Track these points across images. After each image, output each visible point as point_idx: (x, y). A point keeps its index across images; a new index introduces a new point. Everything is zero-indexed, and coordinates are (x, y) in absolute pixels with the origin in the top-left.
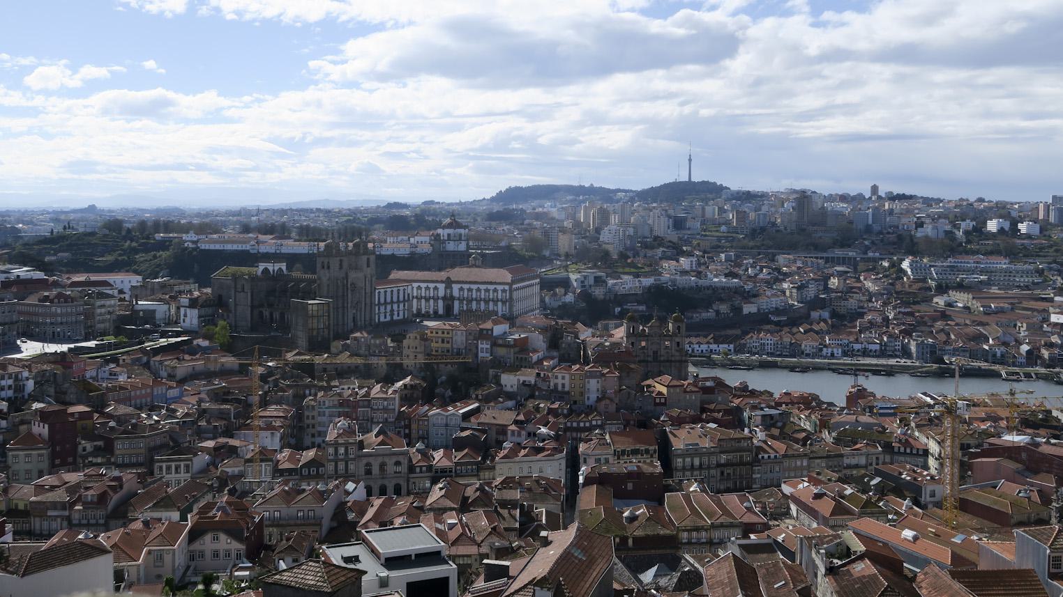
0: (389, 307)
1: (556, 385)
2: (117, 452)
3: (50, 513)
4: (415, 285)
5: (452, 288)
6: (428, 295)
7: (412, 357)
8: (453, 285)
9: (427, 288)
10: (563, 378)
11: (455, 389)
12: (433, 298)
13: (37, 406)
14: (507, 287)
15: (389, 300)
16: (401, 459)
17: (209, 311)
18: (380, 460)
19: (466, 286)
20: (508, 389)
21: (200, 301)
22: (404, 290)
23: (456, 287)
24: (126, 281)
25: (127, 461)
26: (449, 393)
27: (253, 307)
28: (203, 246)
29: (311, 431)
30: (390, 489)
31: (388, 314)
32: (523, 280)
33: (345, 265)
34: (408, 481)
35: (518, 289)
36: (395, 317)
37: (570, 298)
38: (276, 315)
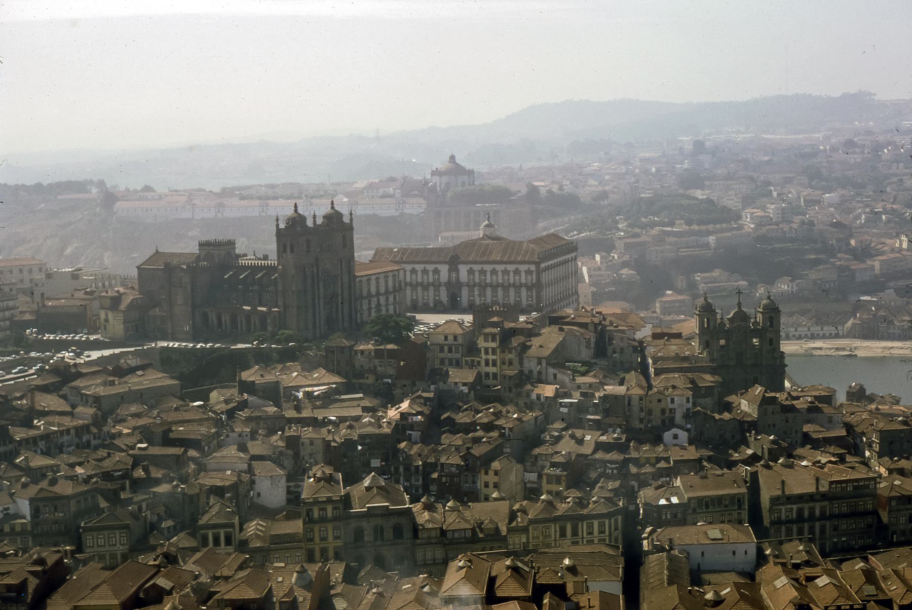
5: (457, 271)
6: (425, 280)
8: (461, 267)
9: (425, 272)
12: (433, 284)
14: (533, 268)
19: (476, 267)
22: (394, 275)
23: (463, 269)
31: (373, 311)
35: (548, 268)
38: (226, 318)
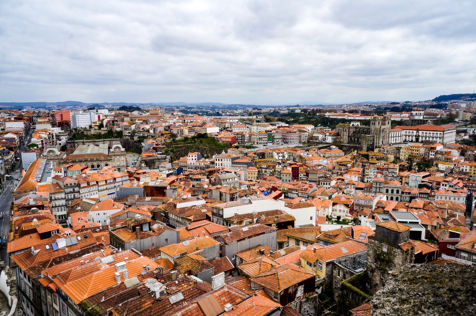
0: (395, 138)
1: (463, 170)
2: (309, 177)
3: (293, 192)
4: (405, 131)
7: (403, 155)
9: (409, 132)
10: (466, 167)
11: (419, 167)
13: (288, 162)
15: (395, 136)
16: (399, 189)
17: (335, 137)
18: (391, 189)
19: (425, 132)
20: (441, 169)
21: (332, 134)
24: (309, 128)
25: (312, 180)
26: (417, 169)
27: (349, 136)
28: (331, 117)
29: (367, 177)
30: (394, 199)
32: (449, 130)
33: (380, 123)
34: (401, 196)
36: (397, 142)
37: (467, 137)
38: (356, 139)
